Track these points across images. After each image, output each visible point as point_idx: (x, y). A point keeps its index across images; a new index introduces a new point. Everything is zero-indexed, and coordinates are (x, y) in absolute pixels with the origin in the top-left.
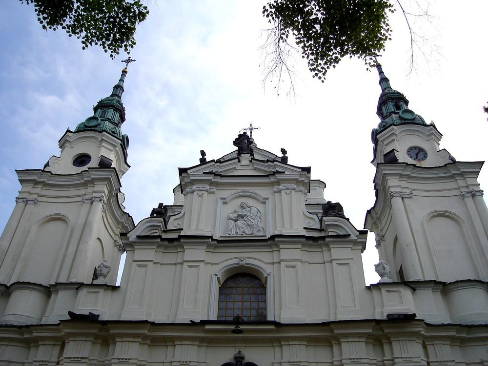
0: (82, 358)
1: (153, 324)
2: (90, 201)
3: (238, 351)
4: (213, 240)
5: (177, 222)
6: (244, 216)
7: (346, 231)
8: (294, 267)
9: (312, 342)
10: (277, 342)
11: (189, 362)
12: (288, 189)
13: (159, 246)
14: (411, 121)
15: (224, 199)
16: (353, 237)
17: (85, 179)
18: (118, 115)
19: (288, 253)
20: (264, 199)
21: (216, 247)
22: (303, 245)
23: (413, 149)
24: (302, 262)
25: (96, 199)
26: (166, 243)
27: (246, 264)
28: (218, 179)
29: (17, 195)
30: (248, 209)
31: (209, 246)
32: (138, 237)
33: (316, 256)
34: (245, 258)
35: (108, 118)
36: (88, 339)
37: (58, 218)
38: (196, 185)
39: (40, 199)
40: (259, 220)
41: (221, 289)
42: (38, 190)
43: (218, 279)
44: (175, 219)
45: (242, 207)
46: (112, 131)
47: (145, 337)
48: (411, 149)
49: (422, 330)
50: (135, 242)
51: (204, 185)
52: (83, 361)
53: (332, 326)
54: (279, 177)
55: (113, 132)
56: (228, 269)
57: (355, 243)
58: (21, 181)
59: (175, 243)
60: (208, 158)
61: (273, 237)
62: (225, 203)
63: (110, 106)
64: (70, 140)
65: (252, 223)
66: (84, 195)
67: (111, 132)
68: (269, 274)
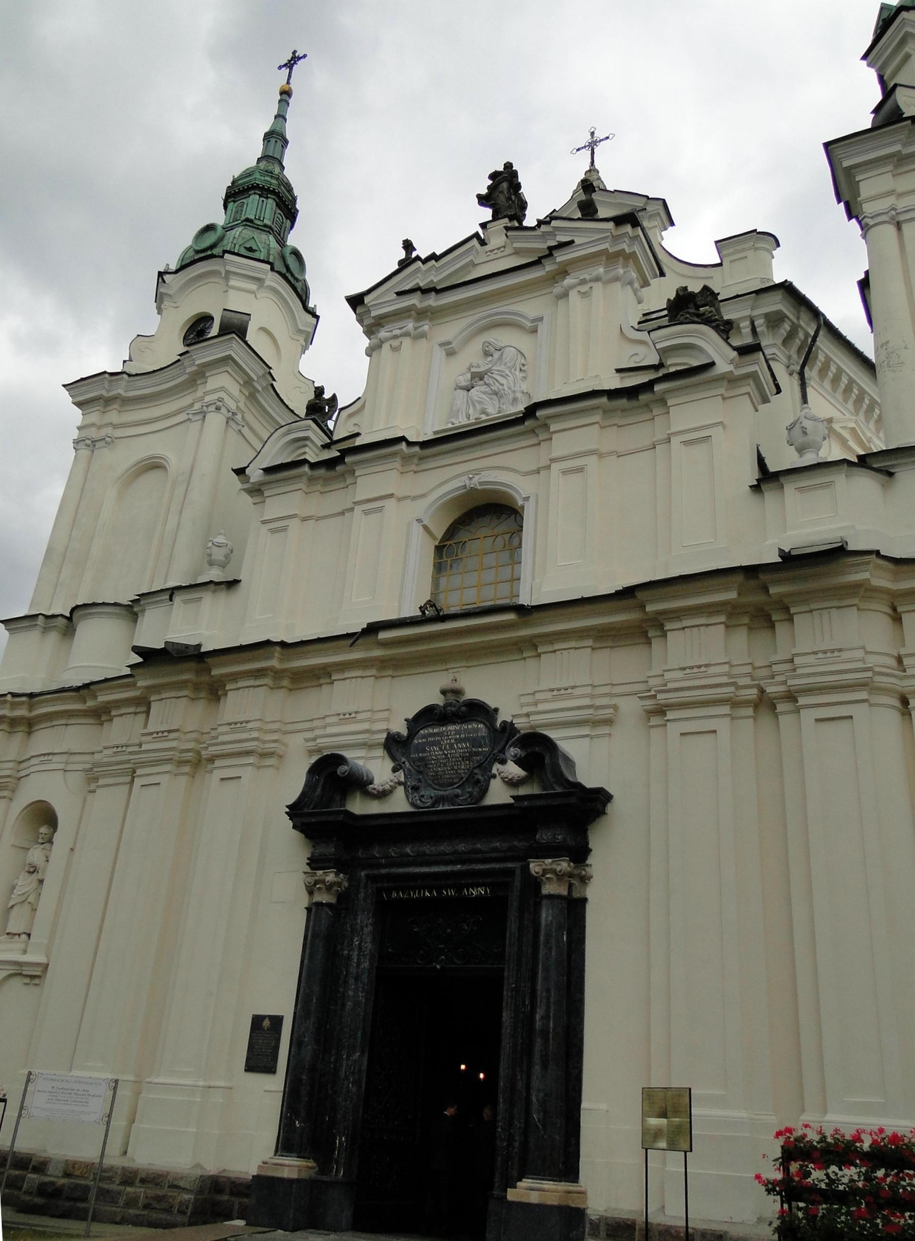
0: (169, 732)
1: (283, 644)
2: (200, 417)
3: (451, 676)
4: (410, 444)
5: (354, 420)
7: (708, 355)
8: (580, 470)
9: (605, 636)
10: (529, 647)
11: (356, 712)
12: (583, 282)
13: (311, 480)
15: (449, 343)
16: (722, 367)
17: (188, 370)
18: (271, 203)
20: (533, 321)
21: (421, 459)
22: (606, 412)
24: (601, 456)
25: (212, 408)
26: (321, 472)
27: (481, 483)
28: (432, 301)
29: (75, 434)
30: (497, 355)
31: (406, 459)
32: (268, 470)
33: (637, 431)
34: (477, 472)
35: (247, 220)
36: (180, 694)
37: (154, 465)
38: (387, 328)
40: (522, 374)
41: (439, 549)
42: (113, 416)
43: (426, 528)
45: (487, 354)
46: (245, 248)
47: (278, 674)
49: (881, 579)
50: (262, 484)
51: (400, 324)
52: (172, 735)
53: (640, 595)
54: (562, 257)
55: (250, 249)
56: (445, 504)
57: (731, 380)
58: (79, 404)
60: (422, 252)
61: (531, 411)
62: (451, 353)
63: (249, 189)
64: (170, 292)
65: (502, 385)
66: (192, 405)
67: (243, 252)
68: (527, 499)
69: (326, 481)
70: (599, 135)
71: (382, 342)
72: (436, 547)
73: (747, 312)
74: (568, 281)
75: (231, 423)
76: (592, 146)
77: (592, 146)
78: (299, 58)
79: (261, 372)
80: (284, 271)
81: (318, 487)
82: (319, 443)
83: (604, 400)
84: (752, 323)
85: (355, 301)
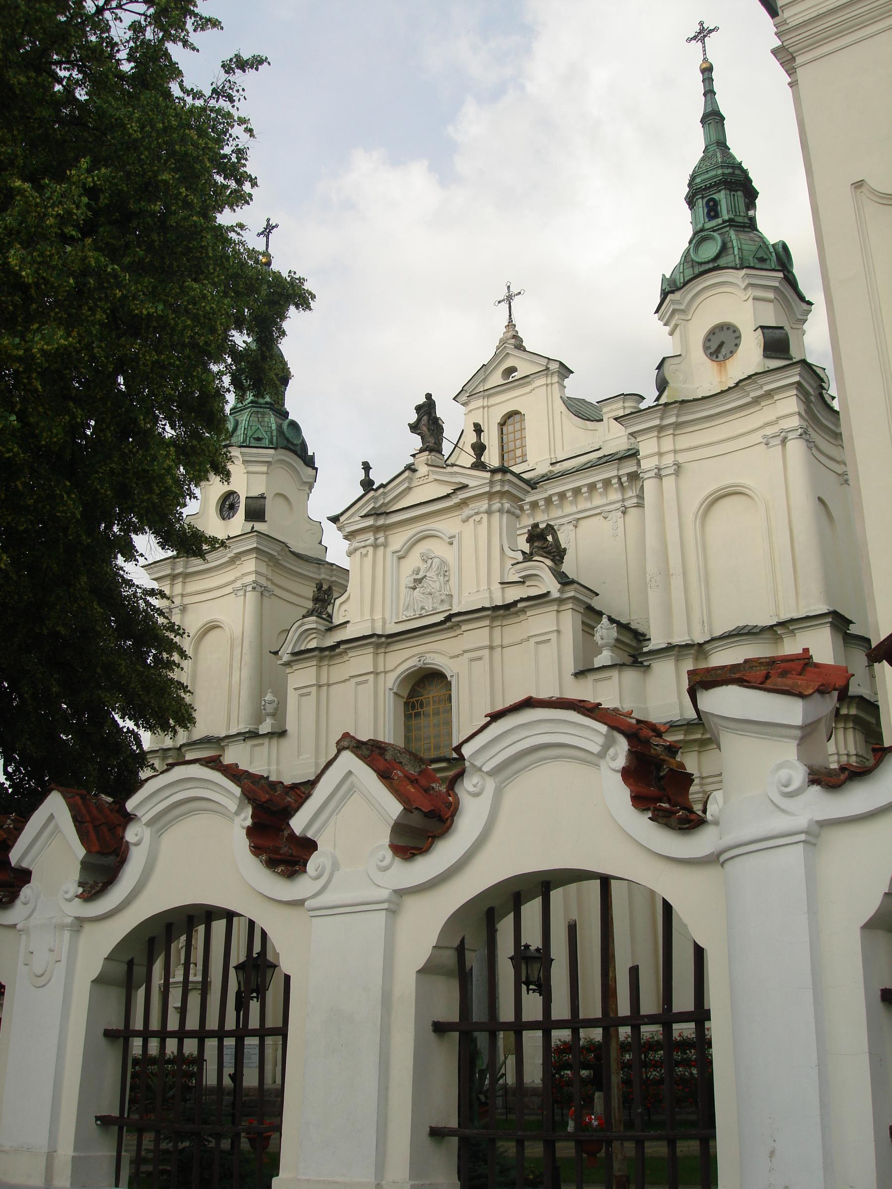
5: (344, 607)
6: (422, 578)
8: (480, 659)
12: (477, 513)
14: (711, 266)
19: (476, 636)
20: (450, 538)
21: (389, 644)
23: (717, 331)
32: (294, 654)
39: (187, 600)
44: (341, 604)
48: (709, 340)
55: (259, 439)
57: (560, 601)
59: (338, 651)
61: (449, 618)
62: (400, 558)
68: (452, 676)
69: (331, 657)
70: (514, 290)
71: (356, 550)
72: (405, 703)
73: (615, 473)
74: (467, 512)
75: (266, 593)
76: (509, 299)
77: (509, 299)
78: (273, 228)
79: (279, 549)
80: (285, 443)
81: (326, 663)
82: (323, 628)
83: (489, 613)
84: (620, 479)
85: (335, 519)
